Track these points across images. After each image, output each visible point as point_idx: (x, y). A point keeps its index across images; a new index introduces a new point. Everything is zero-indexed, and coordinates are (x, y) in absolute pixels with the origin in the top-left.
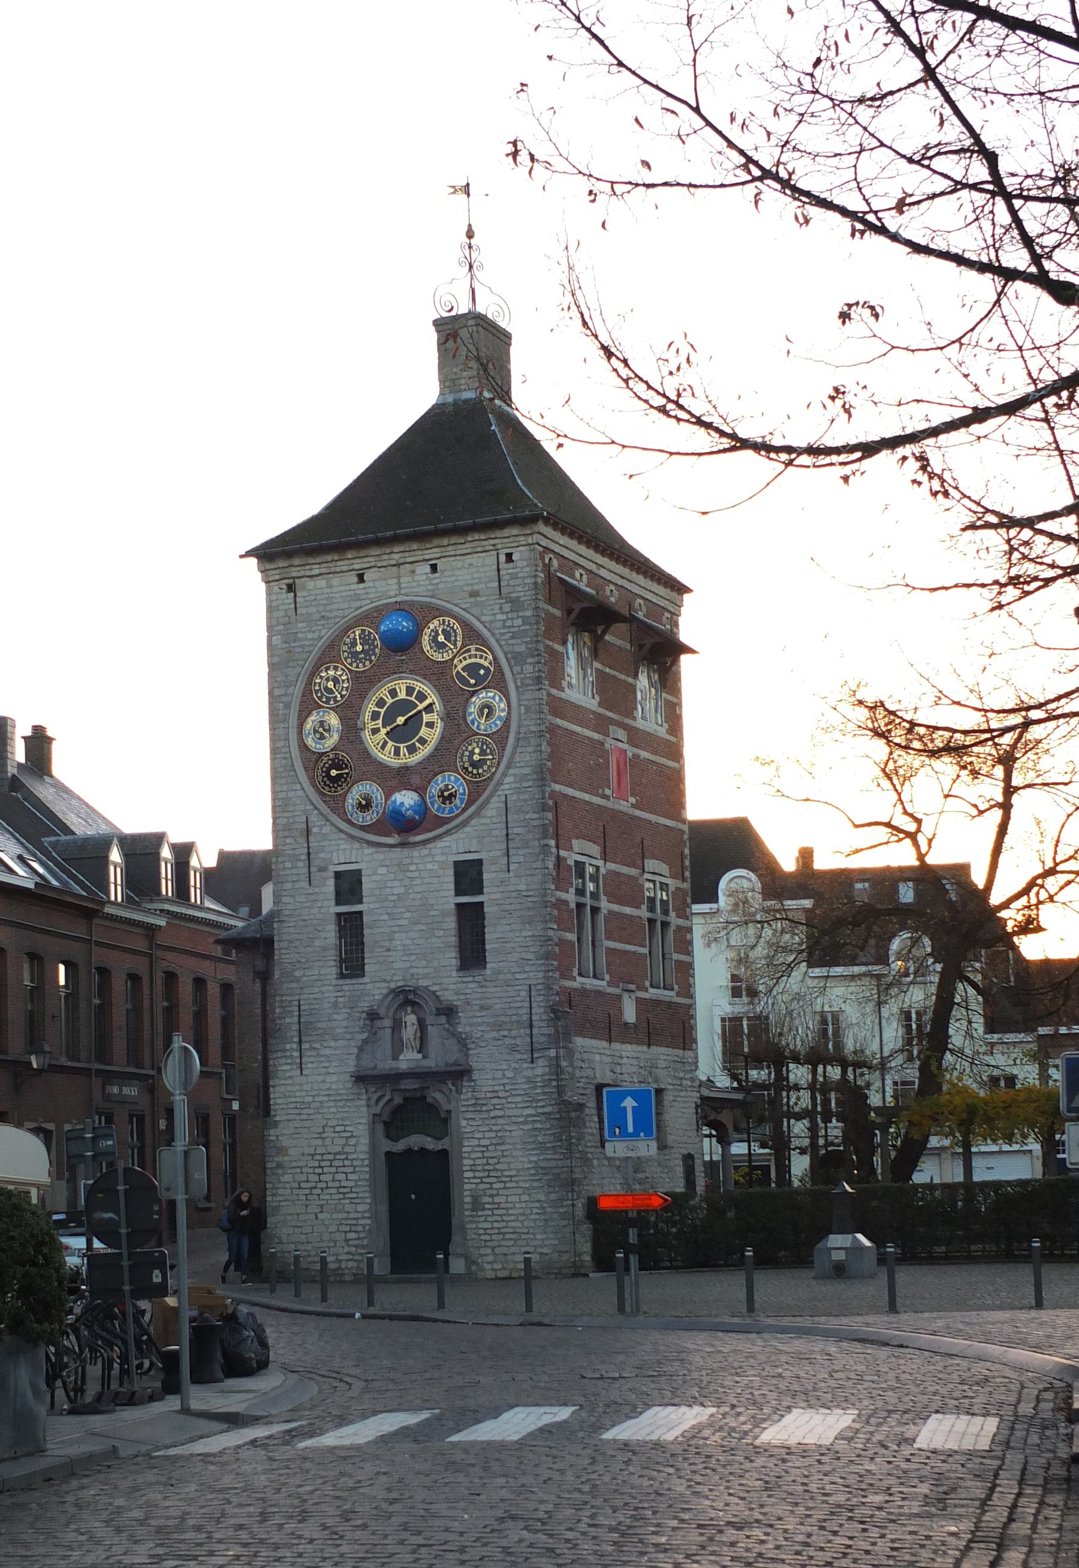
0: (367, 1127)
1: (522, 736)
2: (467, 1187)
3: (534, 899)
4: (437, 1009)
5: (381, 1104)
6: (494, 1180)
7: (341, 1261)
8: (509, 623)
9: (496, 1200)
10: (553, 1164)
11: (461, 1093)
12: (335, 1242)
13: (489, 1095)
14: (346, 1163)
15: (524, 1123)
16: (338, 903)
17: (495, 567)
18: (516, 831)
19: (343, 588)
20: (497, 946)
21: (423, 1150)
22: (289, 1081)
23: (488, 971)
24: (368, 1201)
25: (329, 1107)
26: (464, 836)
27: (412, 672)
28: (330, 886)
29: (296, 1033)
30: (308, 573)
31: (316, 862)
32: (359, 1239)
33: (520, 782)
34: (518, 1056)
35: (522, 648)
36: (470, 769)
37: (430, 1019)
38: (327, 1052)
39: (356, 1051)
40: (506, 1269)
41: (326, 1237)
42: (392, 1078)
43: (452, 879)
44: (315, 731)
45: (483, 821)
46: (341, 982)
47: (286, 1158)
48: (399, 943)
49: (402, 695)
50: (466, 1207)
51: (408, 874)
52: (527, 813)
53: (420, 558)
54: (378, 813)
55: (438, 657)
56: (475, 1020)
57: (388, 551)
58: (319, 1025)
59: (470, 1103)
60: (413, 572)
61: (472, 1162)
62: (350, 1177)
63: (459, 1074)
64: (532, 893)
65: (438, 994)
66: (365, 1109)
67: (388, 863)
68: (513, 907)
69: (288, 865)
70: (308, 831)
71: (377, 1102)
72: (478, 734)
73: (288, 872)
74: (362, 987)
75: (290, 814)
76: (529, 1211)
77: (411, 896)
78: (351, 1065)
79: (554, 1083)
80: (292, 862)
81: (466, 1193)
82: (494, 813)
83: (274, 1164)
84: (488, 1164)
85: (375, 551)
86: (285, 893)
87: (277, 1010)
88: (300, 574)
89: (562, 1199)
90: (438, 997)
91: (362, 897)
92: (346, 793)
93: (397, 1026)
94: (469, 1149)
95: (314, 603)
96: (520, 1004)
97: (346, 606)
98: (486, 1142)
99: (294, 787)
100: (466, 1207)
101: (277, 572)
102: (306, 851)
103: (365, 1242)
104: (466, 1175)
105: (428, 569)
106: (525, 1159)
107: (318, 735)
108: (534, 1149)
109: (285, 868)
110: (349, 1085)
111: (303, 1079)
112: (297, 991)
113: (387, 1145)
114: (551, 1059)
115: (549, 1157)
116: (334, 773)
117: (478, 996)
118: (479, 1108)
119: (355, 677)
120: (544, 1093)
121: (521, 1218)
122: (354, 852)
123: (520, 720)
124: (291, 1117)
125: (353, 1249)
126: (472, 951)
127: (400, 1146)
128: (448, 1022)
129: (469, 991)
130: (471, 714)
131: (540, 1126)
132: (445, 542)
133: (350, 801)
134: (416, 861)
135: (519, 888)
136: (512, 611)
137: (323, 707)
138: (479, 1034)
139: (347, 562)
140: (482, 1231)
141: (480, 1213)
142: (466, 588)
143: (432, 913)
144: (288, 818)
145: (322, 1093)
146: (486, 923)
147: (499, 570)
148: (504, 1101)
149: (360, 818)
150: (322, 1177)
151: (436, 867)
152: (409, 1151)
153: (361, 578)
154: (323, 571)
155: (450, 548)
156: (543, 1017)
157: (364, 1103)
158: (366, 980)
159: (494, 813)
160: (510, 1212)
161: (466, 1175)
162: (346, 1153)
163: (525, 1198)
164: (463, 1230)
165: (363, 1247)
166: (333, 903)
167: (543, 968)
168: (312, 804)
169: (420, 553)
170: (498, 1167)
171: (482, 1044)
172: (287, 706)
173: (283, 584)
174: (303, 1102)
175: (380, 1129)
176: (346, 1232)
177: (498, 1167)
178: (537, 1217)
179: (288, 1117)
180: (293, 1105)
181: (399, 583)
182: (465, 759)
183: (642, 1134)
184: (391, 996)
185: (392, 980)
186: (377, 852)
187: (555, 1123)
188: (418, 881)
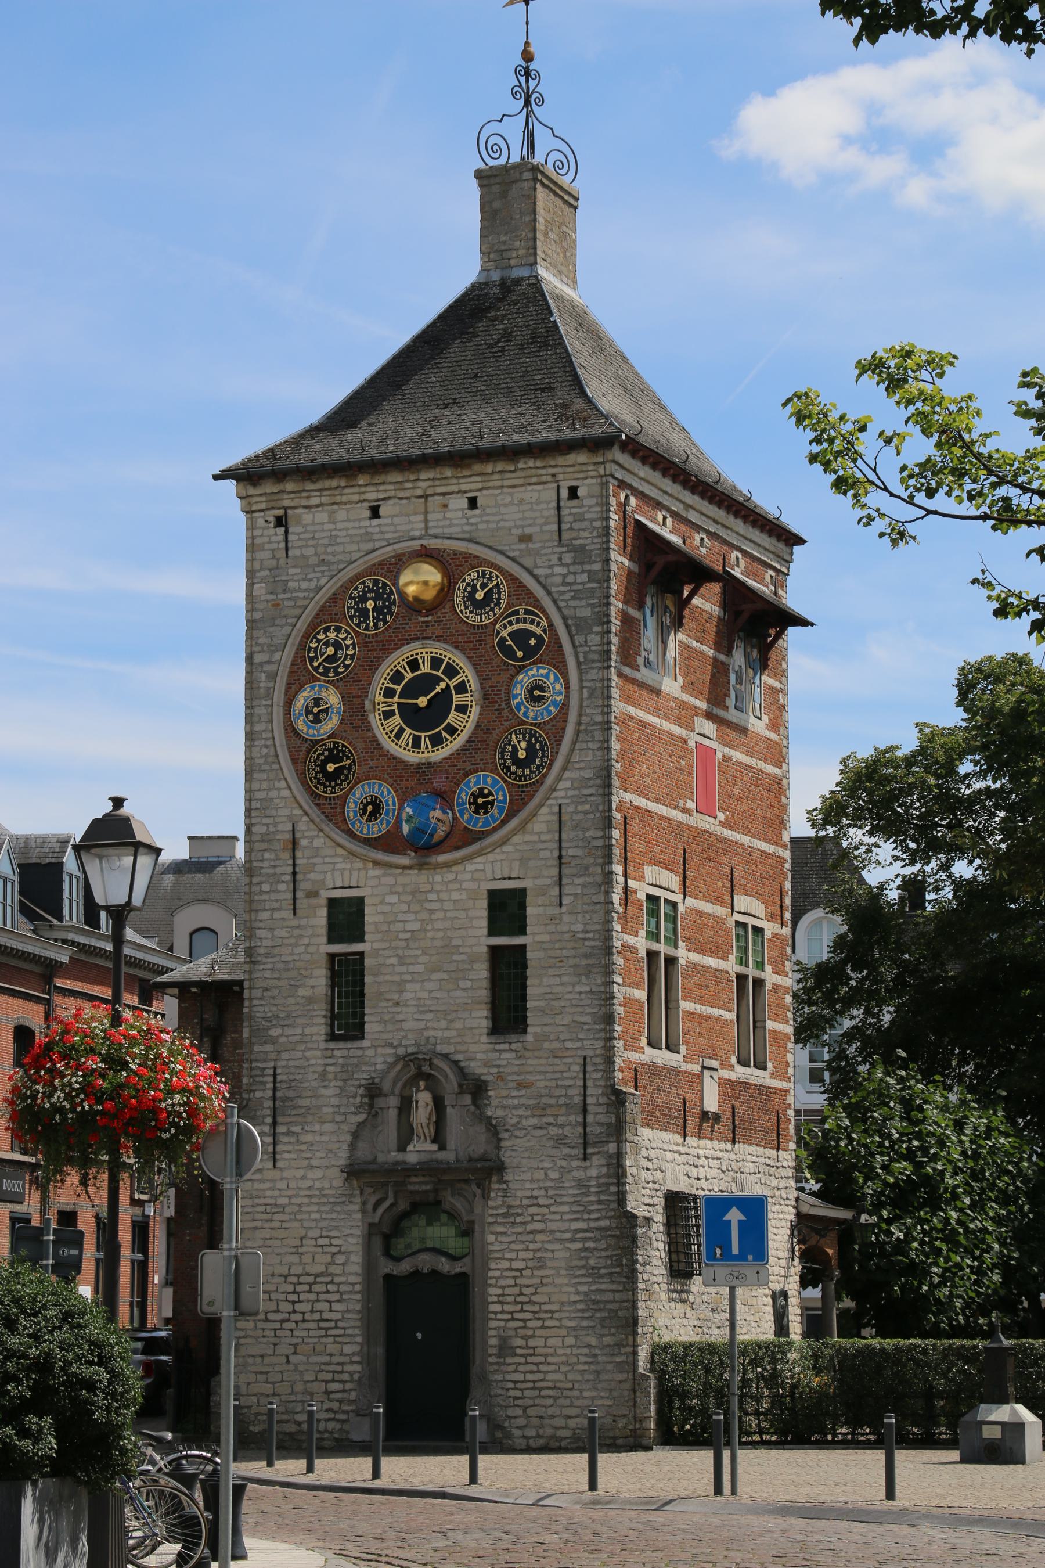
0: (360, 1241)
1: (582, 727)
2: (492, 1324)
3: (592, 943)
4: (460, 1086)
5: (380, 1211)
6: (528, 1316)
8: (570, 579)
9: (532, 1343)
10: (609, 1296)
11: (488, 1198)
12: (312, 1394)
13: (525, 1202)
14: (331, 1288)
15: (572, 1240)
16: (331, 941)
17: (554, 504)
18: (571, 852)
19: (350, 525)
21: (434, 1272)
23: (529, 1037)
24: (359, 1339)
25: (309, 1213)
26: (503, 857)
27: (438, 639)
28: (321, 918)
29: (268, 1112)
30: (304, 502)
31: (303, 886)
32: (344, 1391)
33: (578, 789)
34: (566, 1151)
35: (587, 612)
36: (513, 769)
38: (309, 1138)
39: (349, 1138)
40: (541, 1437)
41: (299, 1387)
42: (393, 1176)
43: (485, 913)
44: (308, 712)
45: (528, 838)
46: (332, 1045)
48: (412, 995)
49: (426, 669)
50: (490, 1351)
51: (427, 905)
52: (588, 829)
53: (455, 488)
54: (388, 822)
55: (475, 620)
56: (510, 1102)
59: (501, 1211)
60: (445, 506)
61: (500, 1291)
62: (336, 1306)
63: (488, 1170)
64: (591, 935)
65: (462, 1064)
66: (359, 1216)
67: (400, 889)
68: (565, 952)
70: (294, 843)
71: (375, 1209)
72: (524, 723)
73: (265, 897)
74: (360, 1053)
76: (575, 1360)
77: (430, 935)
78: (342, 1157)
79: (613, 1189)
81: (491, 1333)
82: (543, 827)
84: (521, 1294)
85: (395, 477)
86: (261, 925)
87: (245, 1080)
88: (292, 504)
89: (619, 1345)
90: (461, 1069)
91: (363, 933)
93: (406, 1106)
94: (497, 1273)
95: (311, 542)
97: (355, 547)
98: (520, 1265)
99: (277, 785)
100: (490, 1351)
101: (263, 499)
102: (290, 869)
103: (353, 1395)
104: (493, 1308)
105: (465, 503)
106: (573, 1290)
107: (311, 717)
109: (261, 892)
110: (338, 1183)
111: (276, 1174)
112: (273, 1056)
115: (603, 1287)
116: (331, 767)
117: (516, 1069)
118: (512, 1219)
119: (365, 642)
120: (599, 1202)
121: (564, 1369)
122: (355, 874)
123: (581, 706)
124: (259, 1224)
125: (335, 1405)
126: (508, 1012)
127: (404, 1267)
128: (474, 1102)
129: (504, 1063)
130: (516, 696)
131: (590, 1244)
132: (489, 468)
133: (352, 805)
134: (438, 887)
135: (574, 928)
136: (574, 563)
137: (319, 680)
138: (515, 1120)
140: (511, 1385)
141: (509, 1360)
142: (514, 531)
143: (455, 957)
144: (267, 825)
146: (528, 972)
147: (559, 508)
148: (545, 1210)
149: (364, 828)
150: (298, 1307)
151: (464, 896)
152: (416, 1274)
153: (375, 513)
154: (324, 499)
155: (496, 477)
156: (601, 1101)
157: (357, 1207)
158: (365, 1043)
159: (543, 827)
161: (493, 1308)
163: (570, 1341)
164: (484, 1378)
165: (351, 1402)
166: (324, 940)
167: (603, 1035)
168: (301, 807)
169: (455, 481)
171: (517, 1133)
172: (272, 677)
173: (271, 516)
175: (378, 1242)
176: (327, 1382)
177: (534, 1298)
178: (586, 1367)
181: (426, 521)
182: (507, 755)
183: (750, 1257)
184: (399, 1067)
185: (400, 1045)
186: (385, 875)
187: (612, 1241)
188: (440, 915)
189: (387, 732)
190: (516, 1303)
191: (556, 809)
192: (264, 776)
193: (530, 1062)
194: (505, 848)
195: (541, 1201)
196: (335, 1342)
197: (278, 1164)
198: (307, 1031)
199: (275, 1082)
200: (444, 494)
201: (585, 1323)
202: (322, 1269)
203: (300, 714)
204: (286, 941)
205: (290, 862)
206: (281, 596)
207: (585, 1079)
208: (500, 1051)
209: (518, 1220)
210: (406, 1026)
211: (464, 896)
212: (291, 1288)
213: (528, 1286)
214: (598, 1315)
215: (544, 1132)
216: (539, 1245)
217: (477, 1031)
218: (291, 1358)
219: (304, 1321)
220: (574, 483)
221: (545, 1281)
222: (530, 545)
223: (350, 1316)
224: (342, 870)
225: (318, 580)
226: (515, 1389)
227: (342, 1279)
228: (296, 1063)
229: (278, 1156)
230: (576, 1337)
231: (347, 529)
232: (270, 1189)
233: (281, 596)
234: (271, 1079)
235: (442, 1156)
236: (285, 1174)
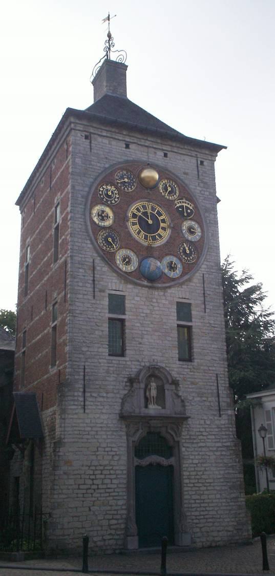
0: (126, 449)
6: (201, 485)
7: (105, 540)
8: (203, 192)
9: (202, 497)
12: (102, 526)
13: (197, 434)
14: (112, 472)
15: (217, 451)
18: (208, 292)
20: (199, 350)
22: (75, 416)
23: (195, 364)
24: (125, 497)
25: (101, 435)
28: (106, 302)
29: (81, 386)
31: (98, 286)
32: (118, 524)
37: (167, 386)
38: (101, 399)
39: (121, 401)
44: (99, 215)
46: (112, 358)
47: (70, 468)
54: (134, 267)
56: (189, 390)
57: (145, 138)
58: (97, 383)
61: (188, 474)
62: (114, 481)
63: (180, 420)
64: (216, 326)
68: (207, 331)
69: (80, 284)
73: (79, 288)
74: (124, 363)
75: (83, 256)
78: (117, 408)
80: (83, 283)
83: (62, 473)
84: (197, 475)
88: (95, 132)
92: (116, 251)
93: (147, 388)
94: (187, 465)
96: (212, 384)
102: (92, 278)
108: (221, 467)
110: (115, 422)
113: (137, 462)
114: (229, 416)
116: (110, 240)
117: (190, 376)
118: (192, 441)
120: (226, 435)
124: (76, 440)
125: (113, 532)
129: (185, 373)
132: (174, 145)
133: (118, 257)
136: (204, 187)
139: (122, 135)
143: (165, 327)
144: (81, 257)
145: (98, 425)
147: (198, 167)
148: (205, 438)
150: (95, 482)
152: (151, 465)
153: (127, 146)
154: (108, 135)
157: (124, 433)
158: (127, 359)
160: (210, 505)
162: (112, 465)
163: (218, 496)
165: (121, 529)
166: (107, 311)
169: (160, 145)
170: (203, 477)
173: (84, 134)
174: (84, 431)
177: (203, 477)
178: (225, 508)
179: (74, 440)
180: (76, 432)
185: (142, 361)
189: (134, 229)
190: (195, 479)
191: (202, 275)
192: (80, 236)
193: (196, 374)
194: (183, 287)
195: (204, 434)
196: (114, 499)
197: (86, 411)
198: (100, 350)
199: (84, 372)
200: (155, 148)
201: (223, 488)
202: (107, 462)
203: (96, 216)
204: (90, 309)
205: (92, 275)
206: (88, 166)
207: (217, 383)
208: (183, 368)
209: (195, 441)
210: (145, 353)
211: (167, 303)
212: (91, 472)
213: (200, 471)
214: (229, 484)
215: (203, 404)
216: (203, 453)
217: (175, 359)
218: (91, 508)
219: (98, 489)
220: (203, 160)
221: (207, 469)
222: (188, 176)
223: (121, 486)
224: (116, 283)
225: (105, 164)
226: (196, 519)
227: (117, 468)
228: (95, 364)
229: (86, 407)
230: (221, 494)
231: (116, 149)
232: (81, 423)
233: (88, 166)
234: (83, 370)
235: (163, 411)
236: (90, 416)
